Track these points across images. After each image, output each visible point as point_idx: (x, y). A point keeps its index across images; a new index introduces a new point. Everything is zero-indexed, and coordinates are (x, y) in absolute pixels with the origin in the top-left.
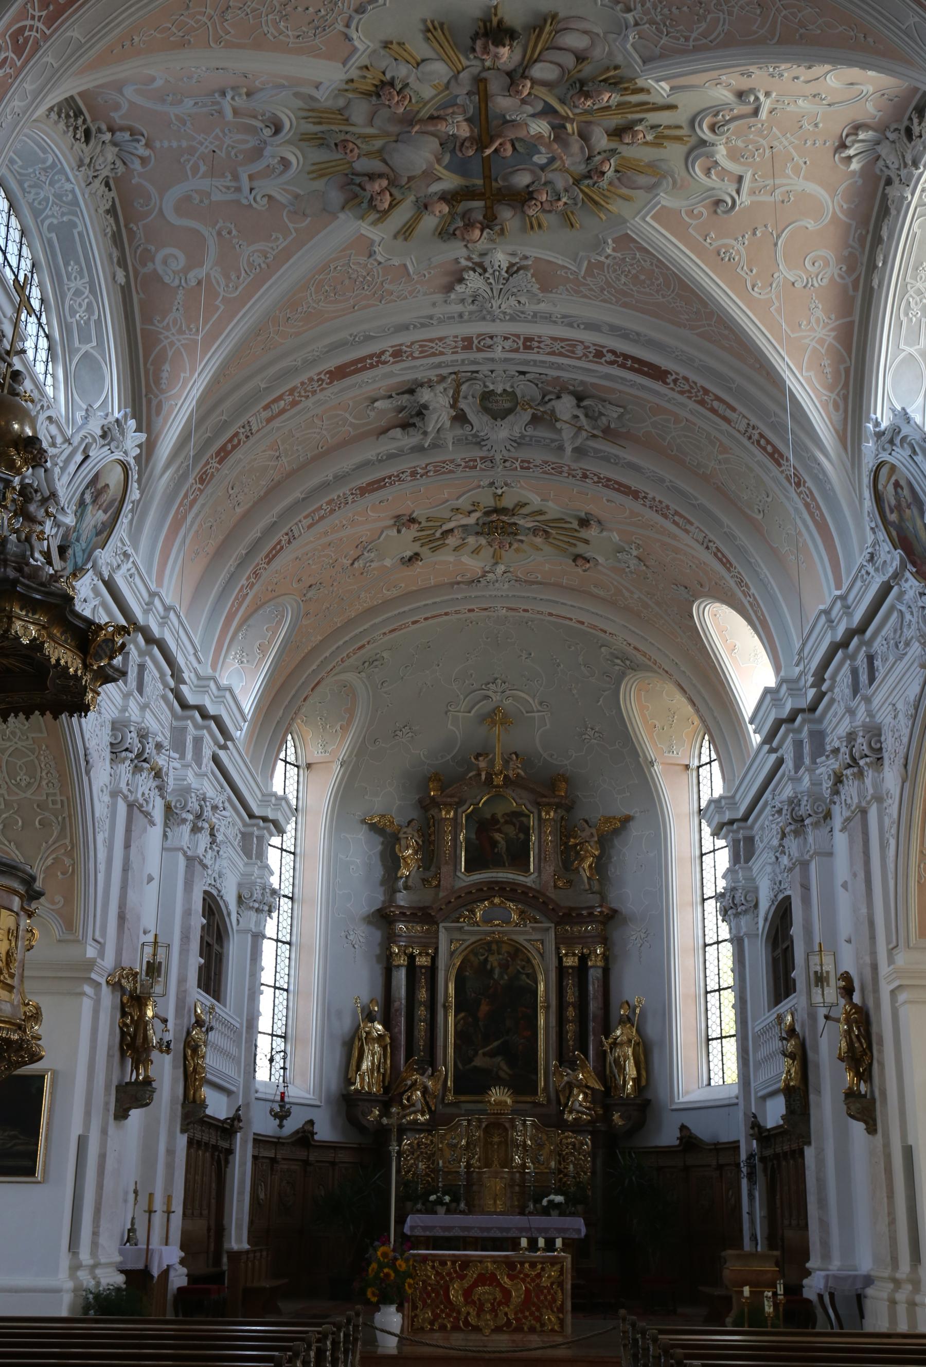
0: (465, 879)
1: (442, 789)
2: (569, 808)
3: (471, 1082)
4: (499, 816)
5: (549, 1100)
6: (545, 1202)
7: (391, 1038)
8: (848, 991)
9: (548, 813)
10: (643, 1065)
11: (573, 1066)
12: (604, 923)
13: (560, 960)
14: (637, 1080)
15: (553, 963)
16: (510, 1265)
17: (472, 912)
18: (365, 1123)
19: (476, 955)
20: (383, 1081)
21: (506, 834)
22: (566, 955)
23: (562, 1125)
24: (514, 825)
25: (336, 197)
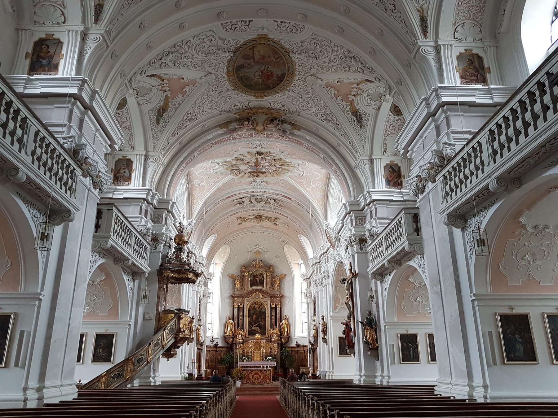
0: (251, 288)
1: (245, 269)
3: (252, 333)
8: (323, 319)
11: (273, 329)
16: (261, 371)
23: (271, 342)
25: (229, 172)
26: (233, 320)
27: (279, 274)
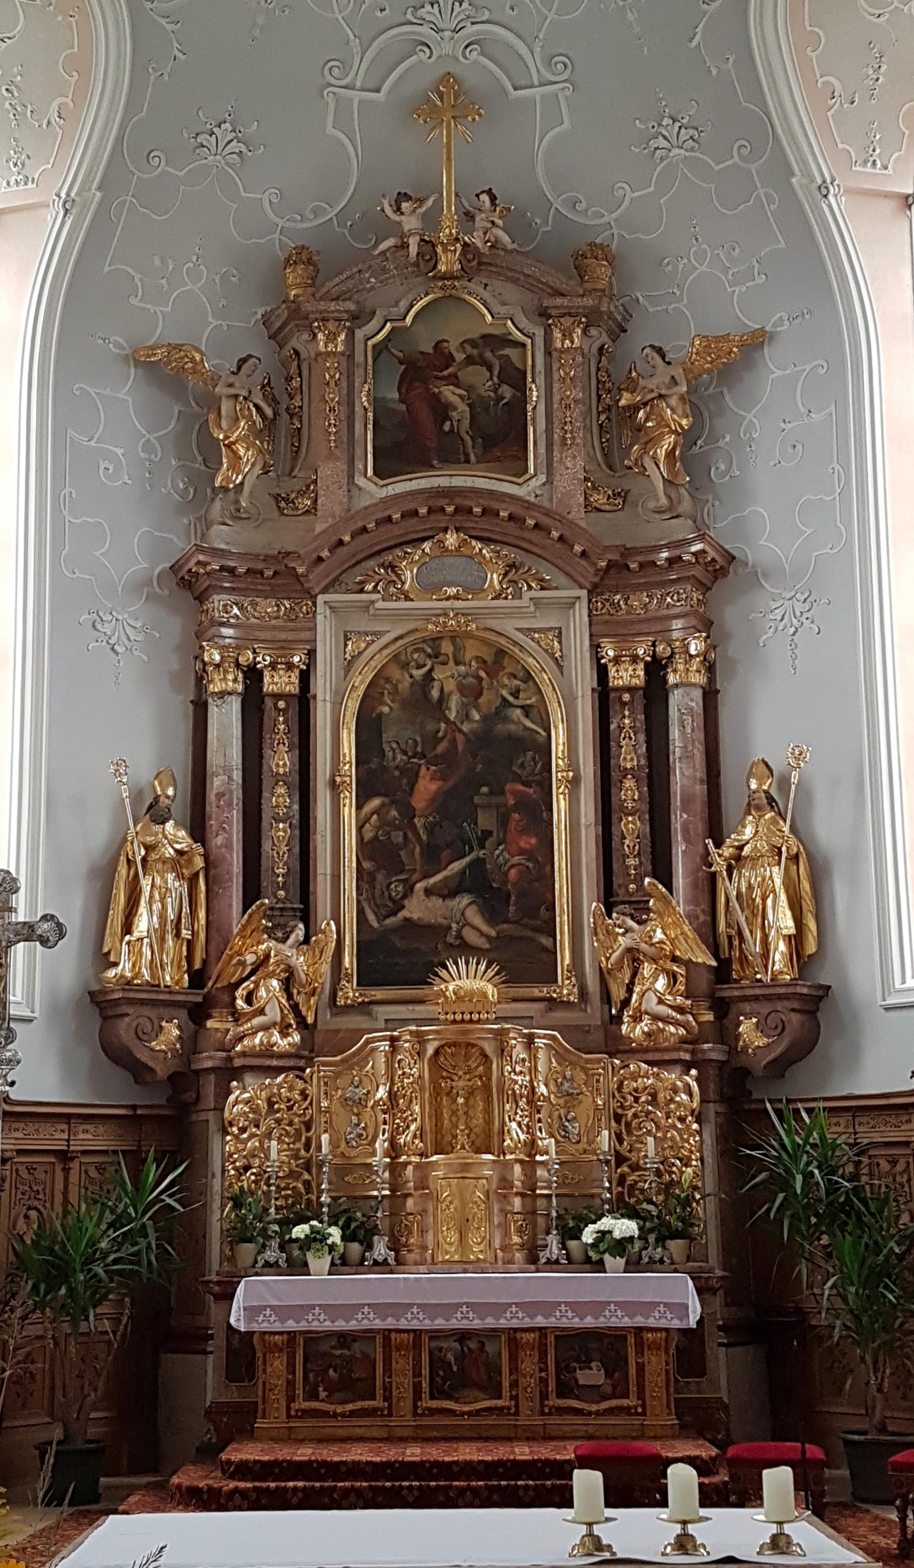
0: (374, 490)
2: (619, 331)
3: (397, 959)
4: (453, 347)
5: (583, 994)
6: (589, 1235)
7: (206, 857)
9: (567, 334)
10: (808, 904)
11: (640, 910)
12: (705, 588)
13: (602, 672)
14: (796, 941)
15: (584, 681)
17: (392, 567)
18: (143, 1056)
19: (405, 666)
20: (190, 958)
21: (470, 389)
22: (616, 660)
23: (616, 1047)
24: (490, 368)
26: (198, 829)
27: (683, 345)
